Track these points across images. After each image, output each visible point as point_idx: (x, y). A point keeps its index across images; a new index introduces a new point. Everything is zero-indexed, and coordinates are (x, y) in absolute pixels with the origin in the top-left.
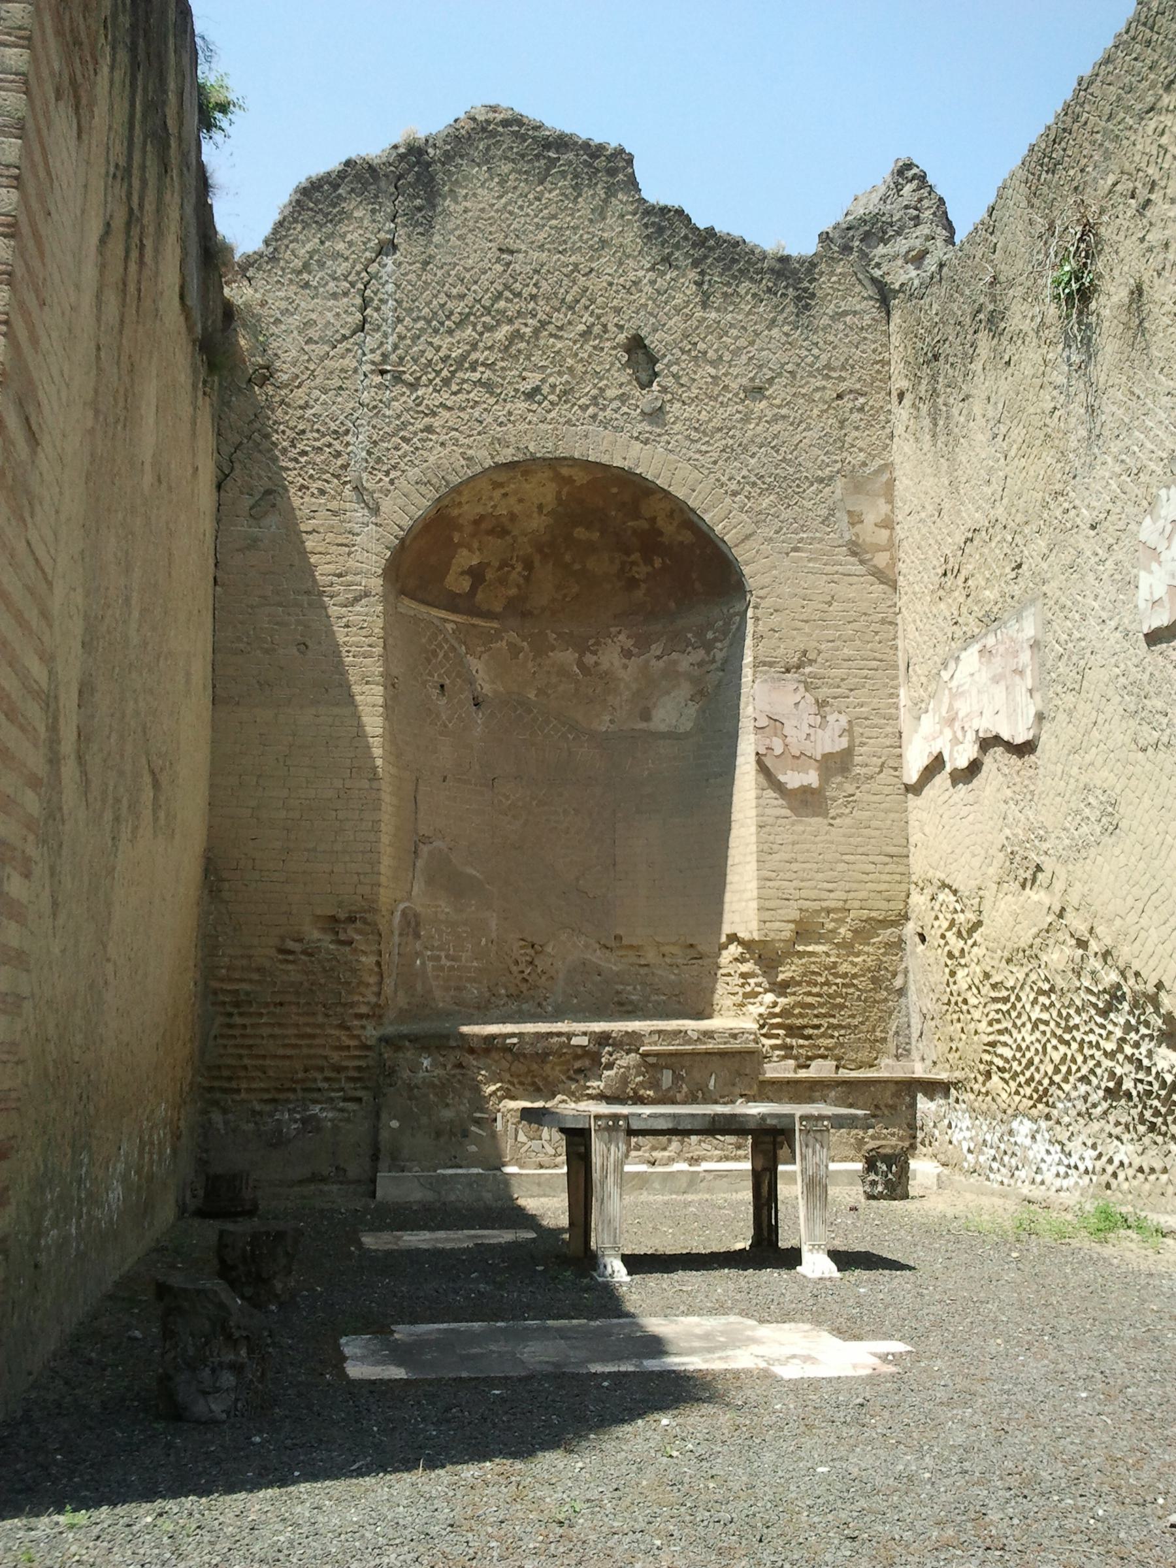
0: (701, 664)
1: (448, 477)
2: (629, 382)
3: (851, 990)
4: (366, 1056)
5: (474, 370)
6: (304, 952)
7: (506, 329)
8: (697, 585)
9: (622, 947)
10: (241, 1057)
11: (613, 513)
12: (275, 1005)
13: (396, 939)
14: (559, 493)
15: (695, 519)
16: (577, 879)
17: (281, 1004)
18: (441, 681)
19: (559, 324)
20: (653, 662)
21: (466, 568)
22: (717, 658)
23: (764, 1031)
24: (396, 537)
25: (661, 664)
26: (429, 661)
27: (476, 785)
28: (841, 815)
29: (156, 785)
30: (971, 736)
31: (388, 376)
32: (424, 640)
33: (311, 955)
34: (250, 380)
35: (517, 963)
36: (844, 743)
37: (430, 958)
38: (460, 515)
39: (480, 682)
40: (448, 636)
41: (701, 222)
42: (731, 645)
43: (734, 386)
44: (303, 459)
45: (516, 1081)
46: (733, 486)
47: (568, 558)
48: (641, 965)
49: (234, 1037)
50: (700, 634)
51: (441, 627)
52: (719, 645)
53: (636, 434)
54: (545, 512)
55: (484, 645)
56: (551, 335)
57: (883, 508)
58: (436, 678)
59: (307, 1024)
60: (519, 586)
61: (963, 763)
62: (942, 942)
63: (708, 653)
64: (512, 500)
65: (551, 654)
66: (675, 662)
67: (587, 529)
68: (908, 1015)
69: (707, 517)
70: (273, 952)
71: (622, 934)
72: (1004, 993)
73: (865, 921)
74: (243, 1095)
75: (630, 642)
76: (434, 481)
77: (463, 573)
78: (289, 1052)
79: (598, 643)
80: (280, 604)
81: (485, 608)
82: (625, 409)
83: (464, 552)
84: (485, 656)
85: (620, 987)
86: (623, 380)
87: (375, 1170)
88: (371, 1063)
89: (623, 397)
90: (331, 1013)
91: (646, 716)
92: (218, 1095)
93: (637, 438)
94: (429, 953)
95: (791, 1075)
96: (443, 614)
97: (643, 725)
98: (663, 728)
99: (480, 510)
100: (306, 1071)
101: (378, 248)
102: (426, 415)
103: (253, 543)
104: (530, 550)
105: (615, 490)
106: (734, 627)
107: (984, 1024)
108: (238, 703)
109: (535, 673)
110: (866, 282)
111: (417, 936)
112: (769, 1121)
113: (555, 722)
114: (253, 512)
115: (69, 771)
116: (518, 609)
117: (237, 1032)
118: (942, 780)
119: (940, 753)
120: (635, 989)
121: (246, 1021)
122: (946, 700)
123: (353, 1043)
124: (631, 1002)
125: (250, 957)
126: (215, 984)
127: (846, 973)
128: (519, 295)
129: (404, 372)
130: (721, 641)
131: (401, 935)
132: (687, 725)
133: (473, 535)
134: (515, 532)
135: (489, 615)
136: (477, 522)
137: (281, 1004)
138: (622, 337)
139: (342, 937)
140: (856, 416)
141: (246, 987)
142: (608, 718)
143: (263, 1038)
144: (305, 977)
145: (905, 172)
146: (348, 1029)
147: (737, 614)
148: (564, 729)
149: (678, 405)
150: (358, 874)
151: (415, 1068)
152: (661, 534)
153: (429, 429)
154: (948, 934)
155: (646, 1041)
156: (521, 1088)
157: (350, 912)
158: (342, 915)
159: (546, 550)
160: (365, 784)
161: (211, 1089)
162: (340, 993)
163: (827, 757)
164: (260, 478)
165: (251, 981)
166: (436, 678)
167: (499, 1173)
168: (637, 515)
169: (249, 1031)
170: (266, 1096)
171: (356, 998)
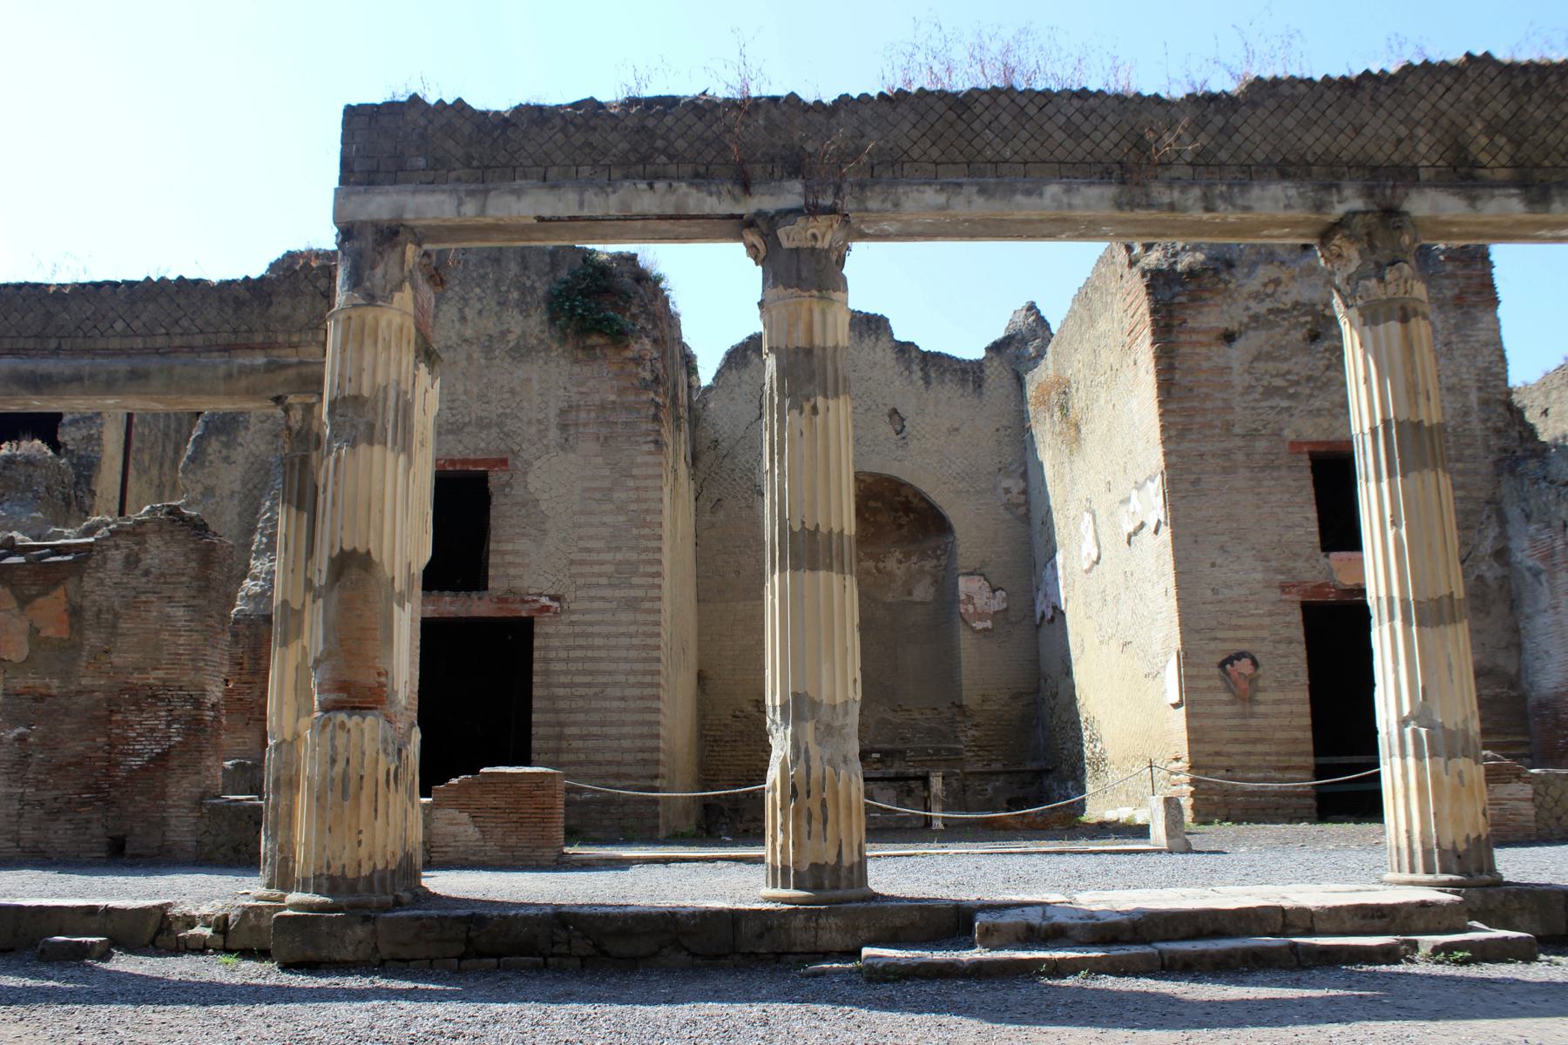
0: (936, 567)
36: (1005, 605)
41: (924, 347)
50: (934, 551)
57: (1022, 484)
91: (910, 593)
98: (918, 599)
103: (713, 525)
118: (1045, 623)
132: (929, 598)
138: (886, 410)
140: (1007, 439)
145: (1032, 307)
149: (915, 442)
163: (996, 613)
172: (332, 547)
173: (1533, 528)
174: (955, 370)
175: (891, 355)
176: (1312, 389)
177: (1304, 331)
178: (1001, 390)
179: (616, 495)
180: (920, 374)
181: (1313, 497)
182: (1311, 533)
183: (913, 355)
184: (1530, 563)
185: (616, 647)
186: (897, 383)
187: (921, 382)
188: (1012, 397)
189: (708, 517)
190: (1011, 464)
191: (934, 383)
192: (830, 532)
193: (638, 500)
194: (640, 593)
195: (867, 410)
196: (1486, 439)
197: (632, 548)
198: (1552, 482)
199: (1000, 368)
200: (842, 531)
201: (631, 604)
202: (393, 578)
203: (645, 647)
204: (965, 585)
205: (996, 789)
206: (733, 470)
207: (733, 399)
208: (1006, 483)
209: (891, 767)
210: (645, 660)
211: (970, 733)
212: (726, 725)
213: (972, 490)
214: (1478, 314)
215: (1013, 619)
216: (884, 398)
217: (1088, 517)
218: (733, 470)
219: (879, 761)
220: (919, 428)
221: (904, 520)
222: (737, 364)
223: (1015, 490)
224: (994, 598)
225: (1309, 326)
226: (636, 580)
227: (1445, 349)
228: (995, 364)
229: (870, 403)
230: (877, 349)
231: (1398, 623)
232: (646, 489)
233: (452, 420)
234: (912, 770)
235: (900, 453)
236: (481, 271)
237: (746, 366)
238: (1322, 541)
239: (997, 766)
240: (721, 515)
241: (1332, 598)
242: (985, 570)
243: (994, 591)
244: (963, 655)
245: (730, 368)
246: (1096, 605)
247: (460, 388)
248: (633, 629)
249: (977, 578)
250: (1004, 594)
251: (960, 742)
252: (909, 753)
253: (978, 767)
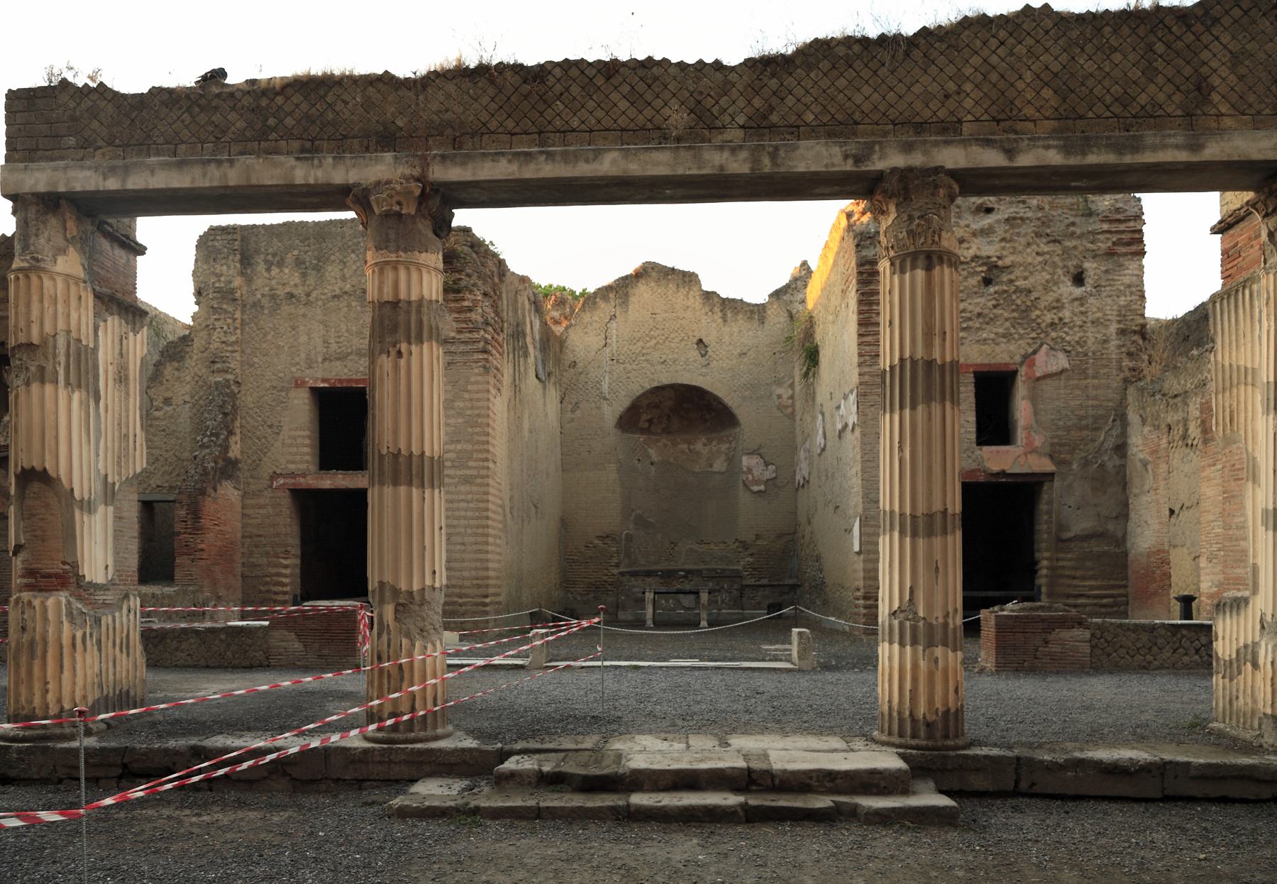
7: (654, 341)
29: (536, 507)
36: (774, 475)
41: (724, 295)
43: (736, 353)
57: (790, 392)
89: (695, 361)
91: (711, 466)
98: (716, 470)
115: (509, 516)
116: (667, 431)
138: (695, 340)
163: (768, 480)
172: (16, 466)
173: (1147, 429)
175: (699, 300)
176: (981, 323)
177: (979, 278)
179: (456, 404)
180: (720, 314)
181: (974, 405)
182: (970, 432)
183: (716, 300)
184: (1141, 456)
185: (458, 509)
186: (703, 321)
187: (720, 320)
189: (569, 415)
192: (411, 454)
193: (472, 408)
194: (474, 472)
196: (1120, 361)
197: (468, 441)
198: (1164, 395)
200: (423, 453)
201: (467, 480)
202: (72, 490)
203: (478, 509)
204: (746, 461)
210: (477, 518)
214: (1126, 263)
217: (820, 417)
223: (785, 396)
225: (983, 274)
226: (471, 464)
227: (1094, 290)
231: (896, 535)
232: (478, 400)
233: (339, 351)
235: (704, 370)
236: (355, 240)
238: (978, 438)
240: (578, 413)
241: (982, 479)
242: (761, 451)
243: (767, 464)
246: (823, 478)
247: (343, 327)
248: (469, 497)
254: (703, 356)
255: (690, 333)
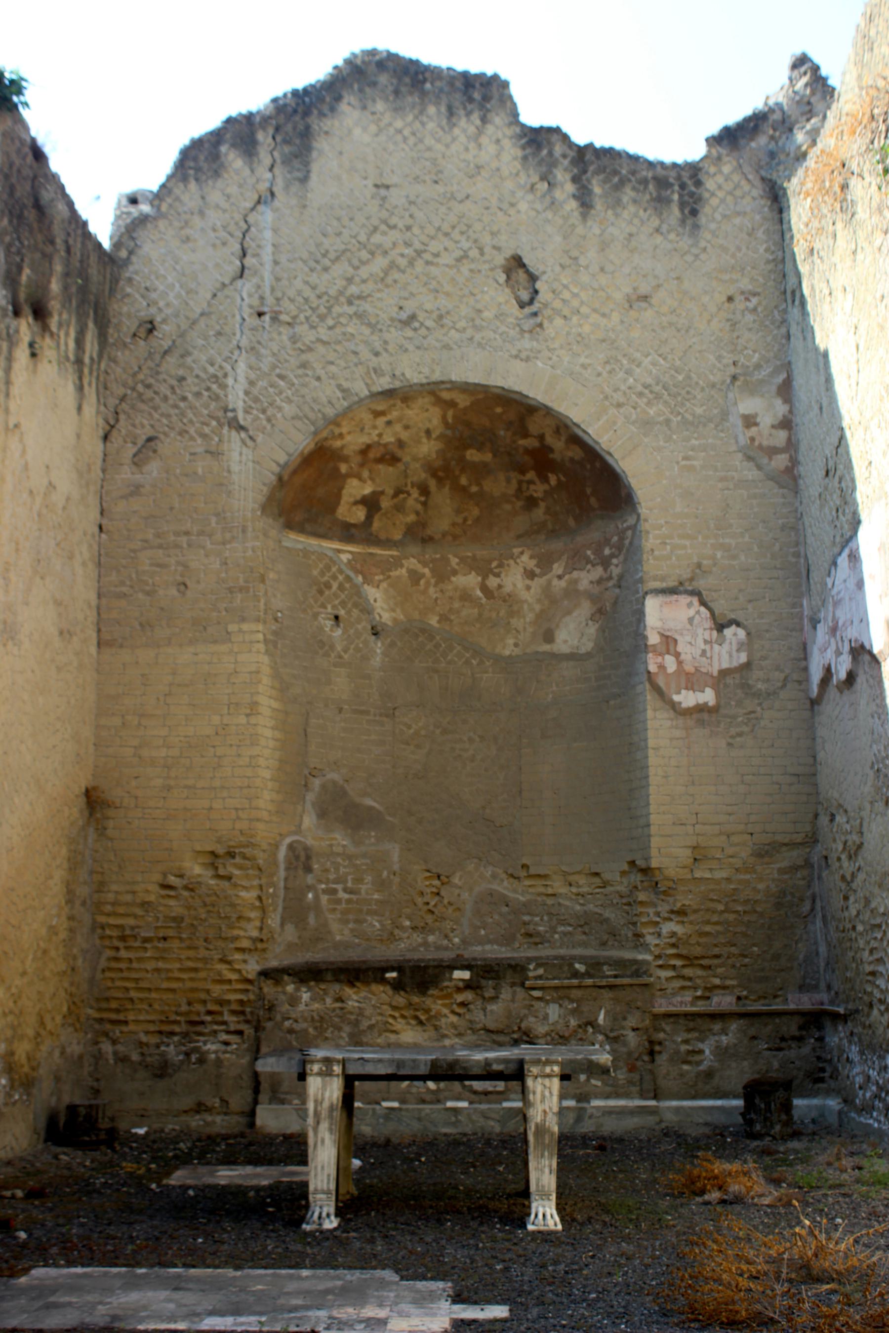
0: (600, 581)
1: (323, 410)
2: (507, 302)
3: (753, 918)
4: (247, 991)
5: (350, 303)
6: (186, 888)
7: (380, 263)
8: (593, 501)
9: (530, 876)
10: (127, 989)
11: (502, 433)
12: (159, 939)
13: (282, 873)
14: (444, 418)
15: (581, 434)
16: (484, 808)
17: (165, 939)
18: (336, 612)
19: (435, 251)
20: (555, 582)
21: (359, 498)
22: (614, 575)
23: (660, 962)
24: (273, 473)
25: (563, 583)
26: (321, 592)
27: (375, 715)
28: (740, 735)
30: (847, 648)
31: (267, 318)
32: (315, 573)
33: (192, 890)
34: (135, 335)
35: (422, 894)
36: (743, 658)
37: (324, 891)
38: (343, 447)
39: (379, 610)
40: (343, 567)
41: (580, 138)
42: (626, 560)
43: (618, 296)
44: (182, 404)
45: (397, 1014)
46: (618, 397)
47: (464, 481)
48: (548, 895)
49: (121, 970)
50: (598, 551)
51: (335, 559)
52: (615, 561)
53: (514, 352)
54: (434, 436)
55: (383, 573)
56: (428, 263)
57: (781, 409)
58: (329, 609)
59: (189, 959)
60: (417, 513)
61: (843, 675)
62: (837, 864)
63: (605, 570)
64: (398, 427)
65: (453, 579)
66: (576, 581)
67: (479, 450)
68: (816, 943)
69: (590, 432)
70: (154, 888)
71: (528, 863)
72: (878, 921)
73: (769, 844)
74: (132, 1027)
75: (534, 562)
76: (312, 415)
77: (356, 503)
78: (174, 985)
79: (501, 566)
80: (160, 547)
81: (383, 536)
82: (503, 329)
83: (354, 482)
84: (384, 585)
85: (526, 918)
86: (501, 299)
87: (256, 1102)
88: (252, 997)
89: (500, 316)
90: (211, 947)
91: (549, 637)
92: (108, 1026)
93: (516, 357)
94: (323, 886)
95: (689, 1009)
96: (336, 545)
97: (546, 647)
98: (565, 649)
99: (364, 439)
100: (189, 1004)
101: (256, 197)
102: (302, 351)
104: (424, 475)
105: (499, 410)
106: (627, 542)
107: (867, 953)
108: (121, 646)
109: (436, 599)
110: (758, 183)
111: (308, 869)
112: (495, 1067)
113: (459, 648)
114: (136, 460)
117: (123, 965)
118: (832, 692)
119: (829, 665)
120: (542, 920)
121: (131, 955)
122: (831, 608)
123: (234, 976)
124: (538, 934)
125: (134, 893)
126: (102, 919)
127: (748, 900)
128: (394, 227)
129: (281, 312)
130: (616, 557)
131: (287, 869)
132: (588, 646)
133: (362, 465)
134: (407, 459)
135: (387, 543)
136: (365, 451)
137: (165, 939)
138: (500, 260)
139: (221, 872)
140: (750, 317)
141: (131, 921)
142: (511, 641)
143: (147, 971)
144: (186, 912)
146: (229, 963)
147: (629, 528)
148: (468, 655)
149: (558, 322)
150: (236, 809)
151: (294, 1001)
152: (551, 450)
153: (304, 365)
154: (843, 857)
155: (531, 974)
156: (403, 1021)
157: (230, 847)
158: (221, 850)
159: (440, 474)
160: (243, 720)
161: (101, 1021)
162: (220, 928)
163: (724, 673)
164: (143, 426)
165: (135, 916)
166: (329, 609)
167: (377, 1107)
168: (526, 435)
169: (135, 965)
170: (152, 1028)
171: (236, 932)
174: (645, 182)
175: (511, 152)
178: (737, 221)
180: (570, 188)
183: (558, 149)
186: (523, 206)
188: (760, 234)
189: (126, 474)
190: (758, 367)
191: (599, 205)
195: (459, 260)
199: (736, 178)
205: (722, 1053)
206: (182, 379)
207: (188, 239)
208: (748, 405)
209: (495, 998)
211: (667, 928)
212: (145, 905)
213: (675, 420)
215: (760, 686)
216: (493, 234)
218: (182, 379)
219: (468, 986)
220: (566, 295)
221: (538, 490)
222: (198, 169)
223: (766, 420)
224: (721, 642)
228: (726, 169)
229: (465, 245)
230: (484, 140)
234: (479, 1056)
235: (527, 343)
237: (217, 174)
239: (723, 1002)
240: (154, 468)
242: (701, 584)
244: (653, 760)
245: (185, 179)
249: (684, 599)
250: (741, 633)
251: (645, 947)
252: (534, 971)
253: (683, 1002)
254: (522, 305)
255: (486, 240)
